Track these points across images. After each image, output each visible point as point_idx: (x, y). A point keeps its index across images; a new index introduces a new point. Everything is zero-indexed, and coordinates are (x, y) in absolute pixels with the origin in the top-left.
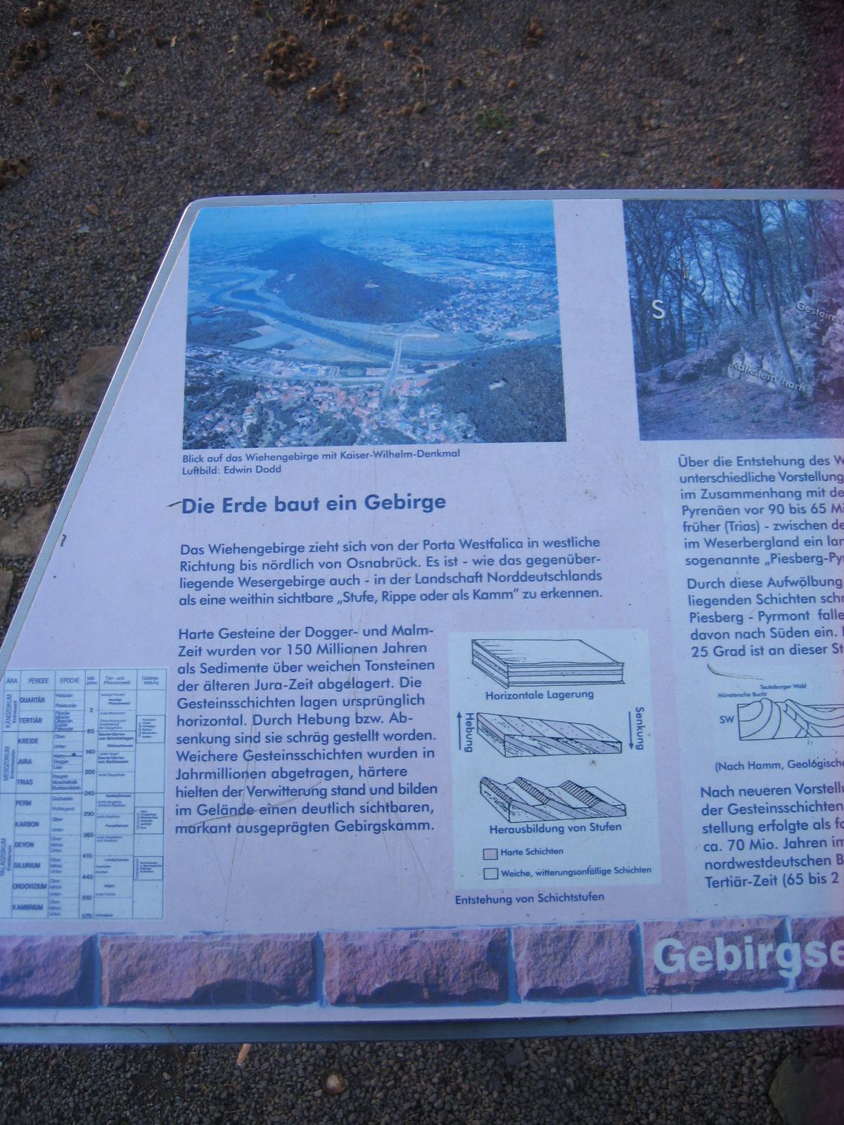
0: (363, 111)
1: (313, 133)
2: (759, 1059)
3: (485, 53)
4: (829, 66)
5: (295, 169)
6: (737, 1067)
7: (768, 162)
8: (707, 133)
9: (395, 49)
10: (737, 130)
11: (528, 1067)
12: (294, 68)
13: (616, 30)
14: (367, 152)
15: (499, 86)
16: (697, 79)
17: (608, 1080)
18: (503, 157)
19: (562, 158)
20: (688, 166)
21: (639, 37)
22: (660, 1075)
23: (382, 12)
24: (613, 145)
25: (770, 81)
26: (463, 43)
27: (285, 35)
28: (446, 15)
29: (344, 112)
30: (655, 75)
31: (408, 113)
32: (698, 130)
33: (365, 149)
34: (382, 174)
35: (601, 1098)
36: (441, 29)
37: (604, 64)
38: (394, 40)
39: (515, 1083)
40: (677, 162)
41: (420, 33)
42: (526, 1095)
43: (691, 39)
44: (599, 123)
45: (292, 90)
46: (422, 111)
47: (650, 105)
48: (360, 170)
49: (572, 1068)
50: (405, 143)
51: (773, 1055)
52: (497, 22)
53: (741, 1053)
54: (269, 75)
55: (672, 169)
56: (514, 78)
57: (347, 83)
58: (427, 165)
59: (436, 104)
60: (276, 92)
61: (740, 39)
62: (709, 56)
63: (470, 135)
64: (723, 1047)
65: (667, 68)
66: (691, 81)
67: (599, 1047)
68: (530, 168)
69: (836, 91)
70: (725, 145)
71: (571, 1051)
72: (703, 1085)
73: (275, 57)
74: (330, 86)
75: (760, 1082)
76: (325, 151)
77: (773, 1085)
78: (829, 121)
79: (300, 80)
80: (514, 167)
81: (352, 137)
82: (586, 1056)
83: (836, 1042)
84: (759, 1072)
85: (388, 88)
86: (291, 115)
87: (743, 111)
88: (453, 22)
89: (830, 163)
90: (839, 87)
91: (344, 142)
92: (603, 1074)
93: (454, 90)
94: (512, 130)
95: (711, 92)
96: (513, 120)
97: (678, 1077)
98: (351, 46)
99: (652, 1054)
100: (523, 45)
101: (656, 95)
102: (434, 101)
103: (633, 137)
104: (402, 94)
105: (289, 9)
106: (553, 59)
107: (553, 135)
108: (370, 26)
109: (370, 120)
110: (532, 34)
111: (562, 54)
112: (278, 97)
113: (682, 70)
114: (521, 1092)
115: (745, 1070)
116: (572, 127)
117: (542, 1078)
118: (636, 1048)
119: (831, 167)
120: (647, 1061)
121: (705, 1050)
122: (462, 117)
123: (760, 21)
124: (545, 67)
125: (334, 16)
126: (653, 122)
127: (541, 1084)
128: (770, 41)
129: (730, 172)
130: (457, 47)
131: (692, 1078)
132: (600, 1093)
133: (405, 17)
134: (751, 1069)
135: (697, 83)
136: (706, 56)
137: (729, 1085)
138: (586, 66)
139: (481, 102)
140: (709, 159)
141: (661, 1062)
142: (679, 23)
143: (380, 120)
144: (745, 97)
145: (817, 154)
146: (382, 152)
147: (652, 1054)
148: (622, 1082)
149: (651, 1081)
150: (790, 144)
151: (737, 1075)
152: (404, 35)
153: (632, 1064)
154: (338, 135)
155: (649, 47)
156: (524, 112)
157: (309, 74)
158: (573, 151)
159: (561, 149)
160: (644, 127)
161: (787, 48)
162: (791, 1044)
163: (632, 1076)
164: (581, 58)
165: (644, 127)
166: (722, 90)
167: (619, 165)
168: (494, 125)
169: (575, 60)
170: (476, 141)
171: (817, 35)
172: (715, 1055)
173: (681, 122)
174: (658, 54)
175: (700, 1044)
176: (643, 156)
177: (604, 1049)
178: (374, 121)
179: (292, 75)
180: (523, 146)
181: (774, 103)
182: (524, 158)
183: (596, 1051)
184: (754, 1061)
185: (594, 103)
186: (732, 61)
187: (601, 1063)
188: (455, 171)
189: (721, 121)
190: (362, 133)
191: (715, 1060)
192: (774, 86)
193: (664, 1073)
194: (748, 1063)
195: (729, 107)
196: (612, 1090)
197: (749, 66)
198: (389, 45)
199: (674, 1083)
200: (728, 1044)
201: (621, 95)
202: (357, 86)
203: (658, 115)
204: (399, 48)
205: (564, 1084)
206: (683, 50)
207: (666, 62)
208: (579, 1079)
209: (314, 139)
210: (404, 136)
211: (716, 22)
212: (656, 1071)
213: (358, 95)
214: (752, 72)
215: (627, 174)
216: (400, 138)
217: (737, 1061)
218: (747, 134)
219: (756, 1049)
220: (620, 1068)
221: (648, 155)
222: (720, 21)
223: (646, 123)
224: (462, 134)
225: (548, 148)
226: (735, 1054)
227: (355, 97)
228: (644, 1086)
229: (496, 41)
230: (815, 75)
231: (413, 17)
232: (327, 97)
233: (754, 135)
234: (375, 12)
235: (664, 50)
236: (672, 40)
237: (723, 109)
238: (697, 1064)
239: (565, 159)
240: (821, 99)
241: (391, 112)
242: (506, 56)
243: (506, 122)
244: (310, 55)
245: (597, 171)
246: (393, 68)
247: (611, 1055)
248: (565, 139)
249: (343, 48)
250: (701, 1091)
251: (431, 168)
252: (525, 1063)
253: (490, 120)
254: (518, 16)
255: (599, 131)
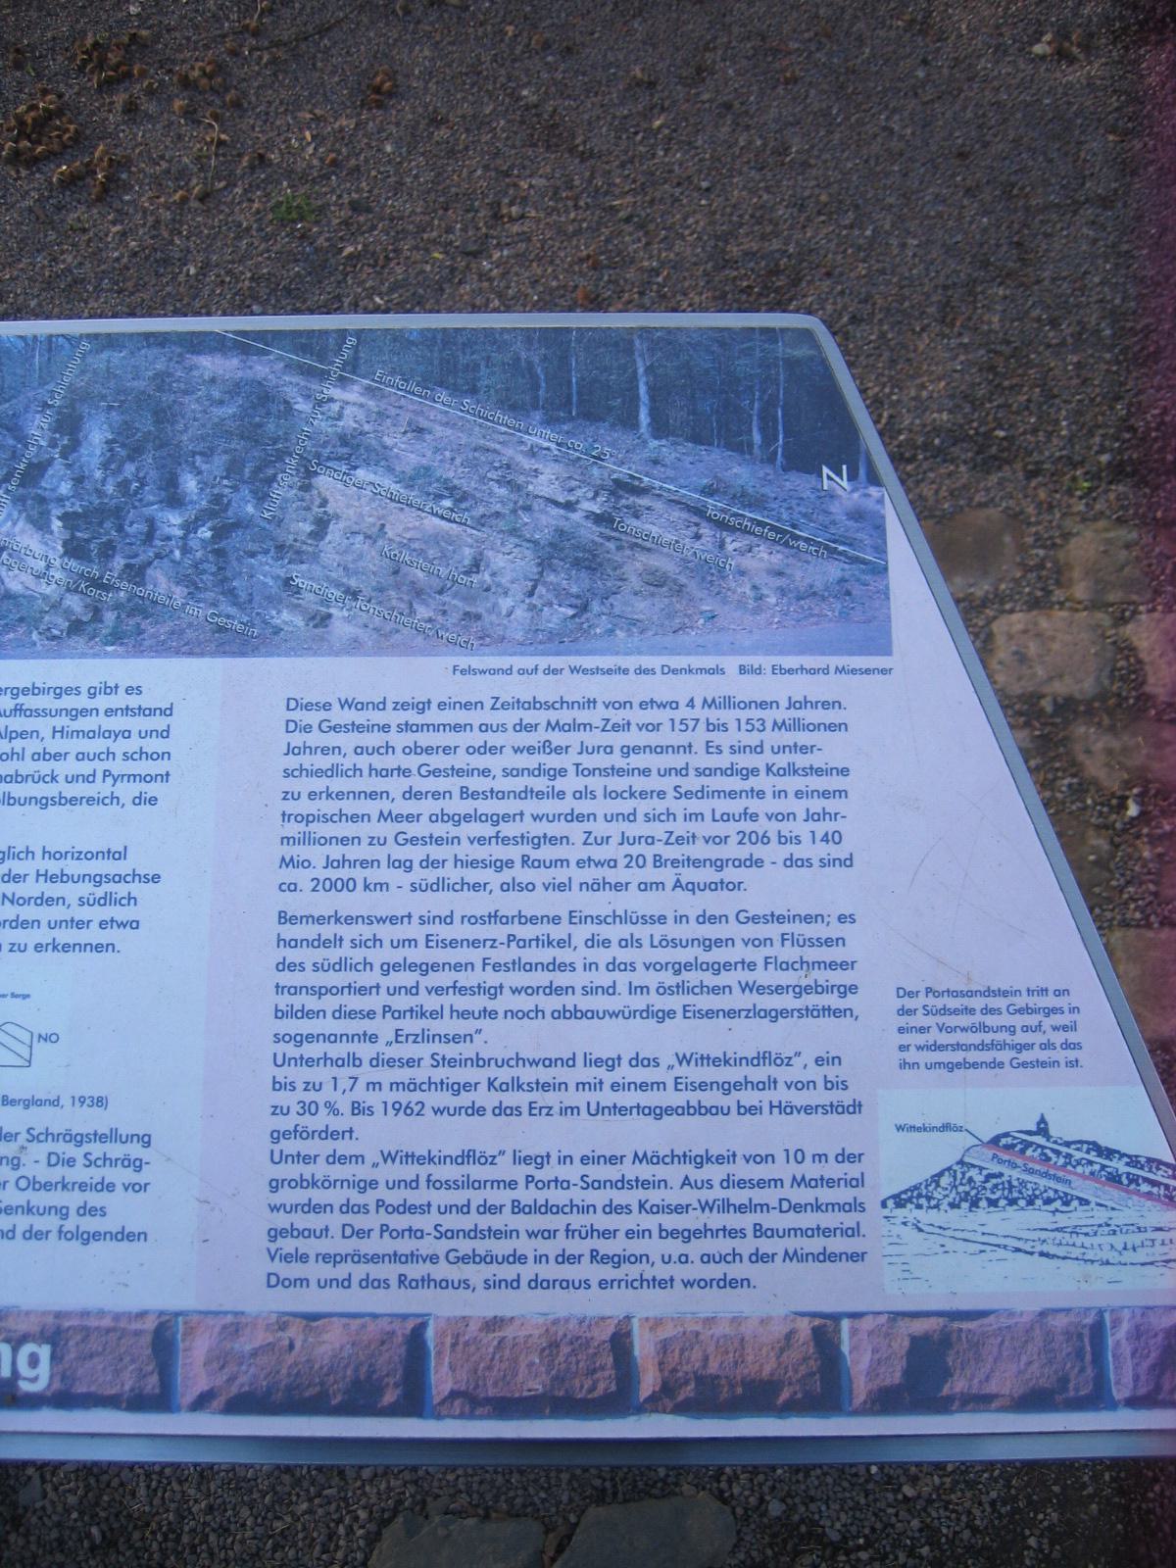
0: (127, 198)
1: (53, 229)
2: (363, 1515)
3: (309, 116)
4: (780, 130)
5: (17, 278)
6: (332, 1525)
7: (663, 264)
8: (585, 225)
9: (189, 113)
10: (628, 220)
11: (43, 1508)
12: (45, 139)
13: (495, 83)
14: (116, 254)
15: (315, 162)
16: (592, 150)
17: (153, 1533)
18: (296, 261)
19: (376, 261)
20: (550, 270)
21: (525, 93)
22: (227, 1530)
23: (184, 61)
24: (451, 242)
25: (693, 152)
26: (281, 103)
27: (45, 92)
28: (266, 65)
29: (99, 199)
30: (535, 145)
31: (184, 200)
32: (574, 220)
33: (117, 250)
34: (130, 284)
35: (138, 1558)
36: (256, 84)
37: (467, 130)
38: (191, 100)
39: (21, 1530)
40: (535, 264)
41: (227, 90)
42: (33, 1547)
43: (596, 94)
44: (440, 212)
45: (39, 170)
46: (203, 198)
47: (515, 185)
48: (102, 279)
49: (102, 1514)
50: (171, 242)
51: (383, 1511)
52: (333, 73)
53: (342, 1504)
54: (11, 148)
55: (527, 274)
56: (339, 153)
57: (111, 159)
58: (192, 271)
59: (225, 188)
60: (18, 172)
61: (666, 93)
62: (614, 117)
63: (260, 230)
64: (319, 1495)
65: (552, 135)
66: (583, 153)
67: (148, 1487)
68: (331, 274)
69: (783, 164)
70: (607, 241)
71: (108, 1490)
72: (283, 1547)
73: (21, 123)
74: (88, 164)
75: (359, 1548)
76: (63, 252)
77: (375, 1552)
78: (762, 207)
79: (50, 156)
80: (310, 274)
81: (101, 234)
82: (128, 1497)
83: (475, 1496)
84: (360, 1532)
85: (164, 165)
86: (28, 203)
87: (646, 194)
88: (275, 75)
89: (752, 264)
90: (788, 159)
91: (90, 240)
92: (148, 1524)
93: (252, 168)
94: (317, 223)
95: (607, 167)
96: (322, 210)
97: (249, 1534)
98: (131, 108)
99: (218, 1501)
100: (362, 105)
101: (528, 172)
102: (223, 184)
103: (484, 230)
104: (183, 174)
105: (60, 58)
106: (398, 124)
107: (374, 228)
108: (161, 82)
109: (131, 211)
110: (377, 90)
111: (410, 116)
112: (19, 178)
113: (574, 138)
114: (28, 1542)
115: (341, 1530)
116: (401, 218)
117: (59, 1525)
118: (199, 1489)
119: (752, 270)
120: (211, 1509)
121: (294, 1498)
122: (256, 205)
123: (699, 70)
124: (384, 134)
125: (118, 65)
126: (514, 209)
127: (54, 1534)
128: (706, 97)
129: (606, 278)
130: (272, 108)
131: (270, 1537)
132: (137, 1550)
133: (208, 69)
134: (350, 1530)
135: (592, 155)
136: (609, 118)
137: (318, 1548)
138: (443, 133)
139: (285, 183)
140: (581, 260)
141: (230, 1512)
142: (584, 74)
143: (145, 211)
144: (652, 174)
145: (734, 250)
146: (135, 254)
147: (218, 1501)
148: (171, 1536)
149: (212, 1538)
150: (699, 238)
151: (330, 1537)
152: (205, 92)
153: (190, 1513)
154: (84, 230)
155: (536, 106)
156: (340, 197)
157: (65, 147)
158: (394, 251)
159: (378, 249)
160: (502, 217)
161: (728, 106)
162: (412, 1496)
163: (186, 1529)
164: (436, 121)
165: (502, 217)
166: (623, 165)
167: (453, 269)
168: (294, 215)
169: (428, 125)
170: (266, 239)
171: (774, 88)
172: (305, 1506)
173: (554, 209)
174: (546, 117)
175: (287, 1489)
176: (491, 257)
177: (155, 1490)
178: (136, 211)
179: (40, 149)
180: (326, 244)
181: (691, 183)
182: (327, 260)
183: (142, 1492)
184: (356, 1519)
185: (439, 184)
186: (645, 125)
187: (147, 1509)
188: (228, 279)
189: (612, 208)
190: (118, 228)
191: (305, 1513)
192: (696, 159)
193: (232, 1527)
194: (347, 1520)
195: (627, 188)
196: (155, 1546)
197: (667, 131)
198: (181, 107)
199: (243, 1542)
200: (326, 1492)
201: (479, 172)
202: (126, 163)
203: (524, 200)
204: (195, 111)
205: (89, 1535)
206: (581, 109)
207: (555, 126)
208: (111, 1529)
209: (52, 236)
210: (171, 233)
211: (637, 72)
212: (221, 1526)
213: (124, 176)
214: (670, 139)
215: (460, 282)
216: (166, 234)
217: (335, 1517)
218: (641, 226)
219: (363, 1502)
220: (171, 1517)
221: (496, 255)
222: (643, 70)
223: (505, 211)
224: (248, 229)
225: (360, 247)
226: (333, 1506)
227: (119, 179)
228: (201, 1544)
229: (327, 99)
230: (759, 143)
231: (220, 68)
232: (82, 178)
233: (652, 227)
234: (174, 62)
235: (555, 111)
236: (569, 97)
237: (617, 191)
238: (279, 1518)
239: (381, 262)
240: (758, 177)
241: (162, 200)
242: (336, 120)
243: (313, 211)
244: (70, 122)
245: (420, 278)
246: (180, 137)
247: (163, 1498)
248: (388, 234)
249: (120, 109)
250: (278, 1555)
251: (197, 275)
252: (38, 1505)
253: (289, 210)
254: (364, 65)
255: (436, 222)
